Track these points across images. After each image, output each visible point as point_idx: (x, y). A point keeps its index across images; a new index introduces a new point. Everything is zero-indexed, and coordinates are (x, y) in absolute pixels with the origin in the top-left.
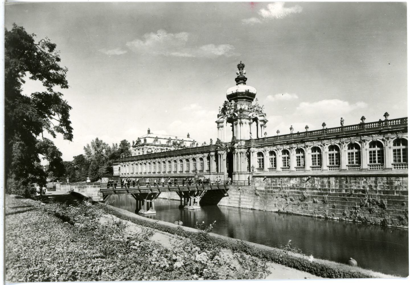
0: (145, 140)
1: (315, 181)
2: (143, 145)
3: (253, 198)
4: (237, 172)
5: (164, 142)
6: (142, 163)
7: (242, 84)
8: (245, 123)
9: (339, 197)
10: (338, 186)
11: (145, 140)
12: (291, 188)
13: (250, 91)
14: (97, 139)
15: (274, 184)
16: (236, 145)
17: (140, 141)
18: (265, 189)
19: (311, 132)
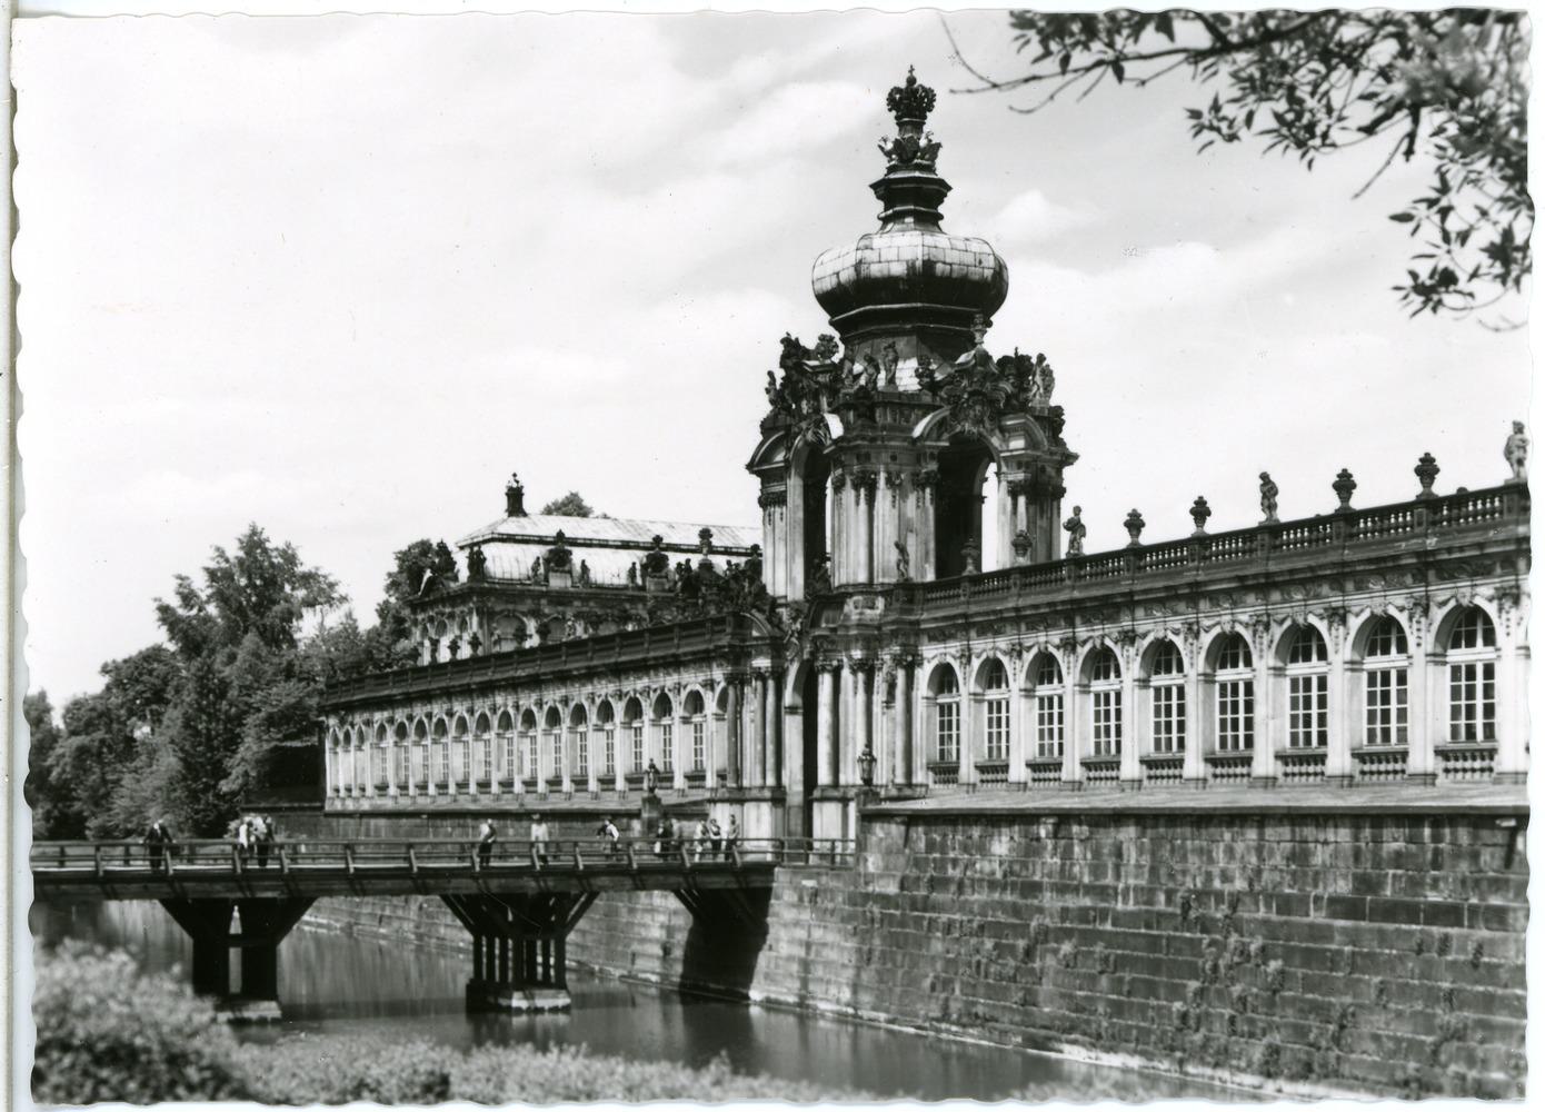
1: (1076, 841)
2: (462, 596)
3: (851, 944)
5: (610, 568)
7: (909, 220)
9: (1143, 931)
10: (1146, 869)
11: (477, 562)
14: (254, 543)
15: (935, 859)
17: (449, 564)
18: (902, 887)
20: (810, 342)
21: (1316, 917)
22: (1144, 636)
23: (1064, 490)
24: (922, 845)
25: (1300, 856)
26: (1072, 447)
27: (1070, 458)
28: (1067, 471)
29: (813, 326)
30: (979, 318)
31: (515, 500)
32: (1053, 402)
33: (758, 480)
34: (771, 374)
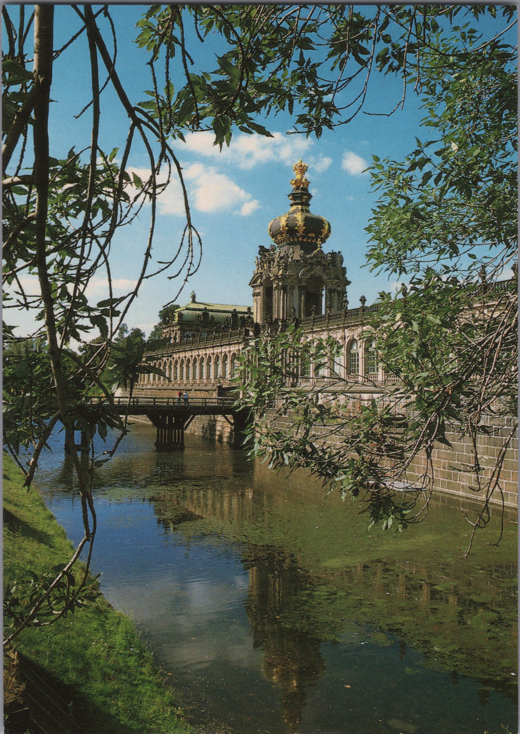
0: (180, 315)
20: (267, 247)
26: (349, 279)
27: (349, 283)
28: (348, 287)
29: (268, 242)
31: (194, 297)
32: (343, 266)
33: (252, 289)
34: (257, 257)
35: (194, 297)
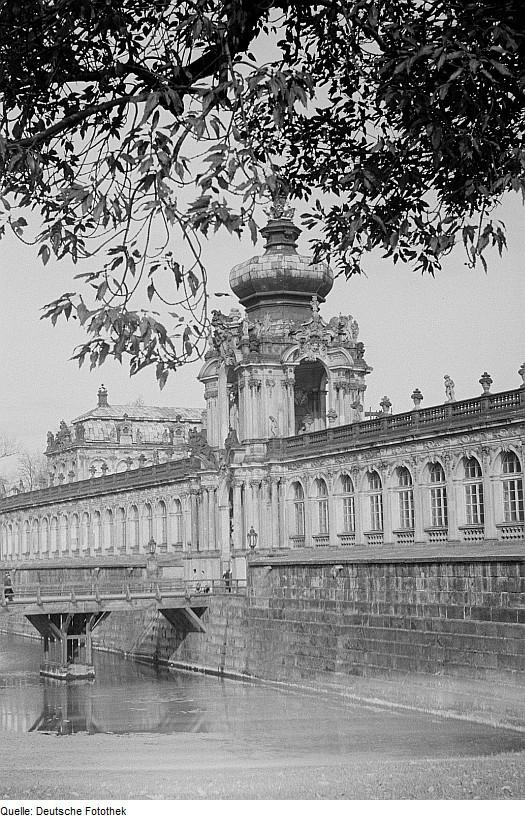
4: (244, 550)
5: (153, 432)
6: (49, 516)
7: (279, 247)
8: (268, 384)
11: (80, 431)
12: (315, 604)
13: (294, 273)
16: (238, 456)
19: (399, 417)
21: (467, 619)
22: (391, 465)
23: (366, 387)
24: (278, 582)
25: (458, 585)
29: (231, 305)
30: (315, 298)
31: (103, 395)
35: (103, 395)
